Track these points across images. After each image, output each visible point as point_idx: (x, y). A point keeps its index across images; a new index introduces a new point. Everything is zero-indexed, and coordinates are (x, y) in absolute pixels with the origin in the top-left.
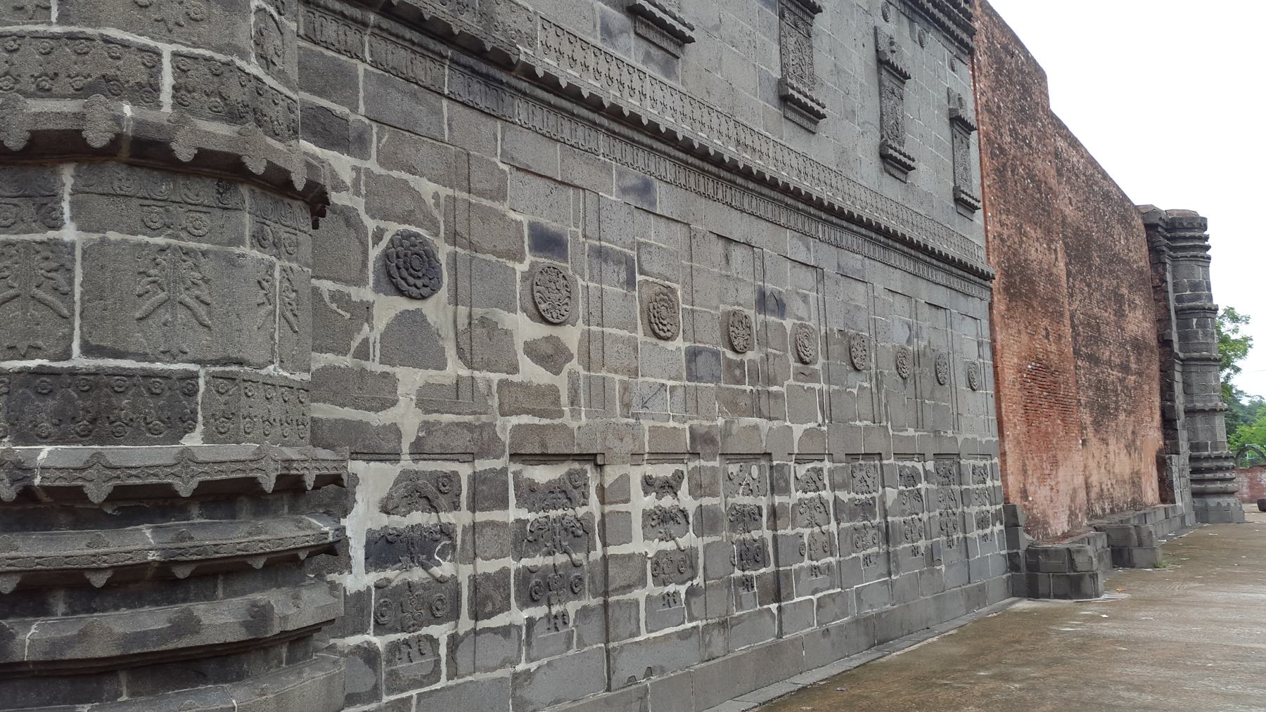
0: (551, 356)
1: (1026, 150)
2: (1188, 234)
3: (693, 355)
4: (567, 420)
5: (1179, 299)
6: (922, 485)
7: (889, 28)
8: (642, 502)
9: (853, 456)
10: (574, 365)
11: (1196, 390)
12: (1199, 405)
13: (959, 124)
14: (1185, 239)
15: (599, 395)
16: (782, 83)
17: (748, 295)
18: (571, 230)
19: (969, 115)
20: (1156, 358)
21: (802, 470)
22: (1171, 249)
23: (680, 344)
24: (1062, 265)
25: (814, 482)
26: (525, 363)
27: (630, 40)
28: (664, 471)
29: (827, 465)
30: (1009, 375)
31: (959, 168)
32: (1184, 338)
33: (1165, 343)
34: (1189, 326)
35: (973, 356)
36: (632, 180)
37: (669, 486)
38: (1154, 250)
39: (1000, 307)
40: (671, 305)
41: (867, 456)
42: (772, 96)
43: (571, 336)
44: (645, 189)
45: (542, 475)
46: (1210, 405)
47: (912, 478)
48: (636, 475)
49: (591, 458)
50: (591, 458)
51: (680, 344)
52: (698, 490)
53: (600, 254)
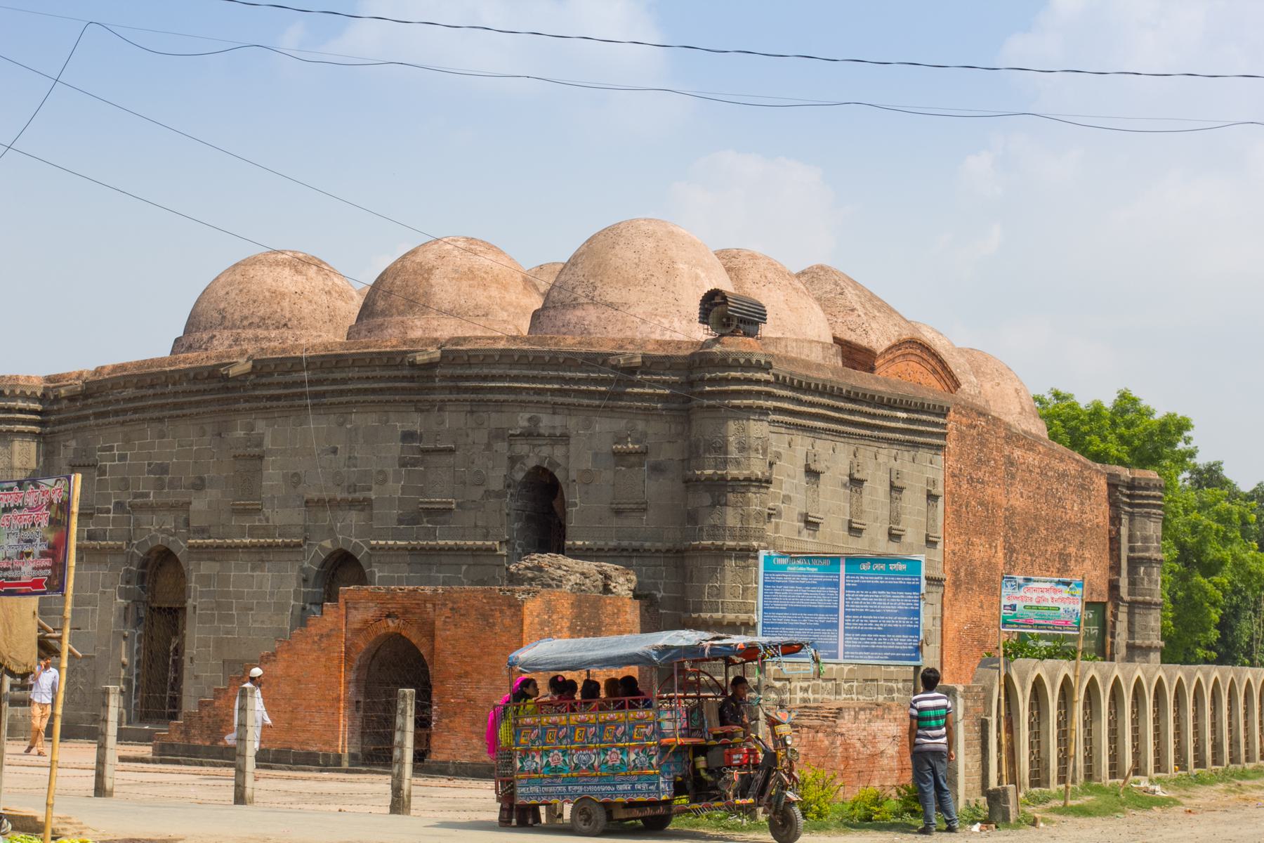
1: (979, 486)
2: (1145, 493)
5: (1132, 549)
6: (895, 695)
7: (896, 465)
8: (800, 695)
9: (866, 680)
11: (1137, 629)
12: (1138, 642)
13: (932, 497)
14: (1142, 497)
19: (939, 490)
21: (846, 686)
22: (1130, 505)
24: (1000, 554)
25: (850, 691)
27: (805, 532)
28: (805, 684)
29: (855, 684)
30: (950, 635)
31: (930, 521)
32: (1132, 583)
34: (1137, 573)
35: (929, 626)
37: (806, 690)
38: (1114, 504)
39: (949, 595)
41: (872, 680)
45: (778, 684)
46: (1147, 642)
47: (890, 691)
48: (799, 684)
49: (788, 680)
50: (788, 680)
52: (814, 692)
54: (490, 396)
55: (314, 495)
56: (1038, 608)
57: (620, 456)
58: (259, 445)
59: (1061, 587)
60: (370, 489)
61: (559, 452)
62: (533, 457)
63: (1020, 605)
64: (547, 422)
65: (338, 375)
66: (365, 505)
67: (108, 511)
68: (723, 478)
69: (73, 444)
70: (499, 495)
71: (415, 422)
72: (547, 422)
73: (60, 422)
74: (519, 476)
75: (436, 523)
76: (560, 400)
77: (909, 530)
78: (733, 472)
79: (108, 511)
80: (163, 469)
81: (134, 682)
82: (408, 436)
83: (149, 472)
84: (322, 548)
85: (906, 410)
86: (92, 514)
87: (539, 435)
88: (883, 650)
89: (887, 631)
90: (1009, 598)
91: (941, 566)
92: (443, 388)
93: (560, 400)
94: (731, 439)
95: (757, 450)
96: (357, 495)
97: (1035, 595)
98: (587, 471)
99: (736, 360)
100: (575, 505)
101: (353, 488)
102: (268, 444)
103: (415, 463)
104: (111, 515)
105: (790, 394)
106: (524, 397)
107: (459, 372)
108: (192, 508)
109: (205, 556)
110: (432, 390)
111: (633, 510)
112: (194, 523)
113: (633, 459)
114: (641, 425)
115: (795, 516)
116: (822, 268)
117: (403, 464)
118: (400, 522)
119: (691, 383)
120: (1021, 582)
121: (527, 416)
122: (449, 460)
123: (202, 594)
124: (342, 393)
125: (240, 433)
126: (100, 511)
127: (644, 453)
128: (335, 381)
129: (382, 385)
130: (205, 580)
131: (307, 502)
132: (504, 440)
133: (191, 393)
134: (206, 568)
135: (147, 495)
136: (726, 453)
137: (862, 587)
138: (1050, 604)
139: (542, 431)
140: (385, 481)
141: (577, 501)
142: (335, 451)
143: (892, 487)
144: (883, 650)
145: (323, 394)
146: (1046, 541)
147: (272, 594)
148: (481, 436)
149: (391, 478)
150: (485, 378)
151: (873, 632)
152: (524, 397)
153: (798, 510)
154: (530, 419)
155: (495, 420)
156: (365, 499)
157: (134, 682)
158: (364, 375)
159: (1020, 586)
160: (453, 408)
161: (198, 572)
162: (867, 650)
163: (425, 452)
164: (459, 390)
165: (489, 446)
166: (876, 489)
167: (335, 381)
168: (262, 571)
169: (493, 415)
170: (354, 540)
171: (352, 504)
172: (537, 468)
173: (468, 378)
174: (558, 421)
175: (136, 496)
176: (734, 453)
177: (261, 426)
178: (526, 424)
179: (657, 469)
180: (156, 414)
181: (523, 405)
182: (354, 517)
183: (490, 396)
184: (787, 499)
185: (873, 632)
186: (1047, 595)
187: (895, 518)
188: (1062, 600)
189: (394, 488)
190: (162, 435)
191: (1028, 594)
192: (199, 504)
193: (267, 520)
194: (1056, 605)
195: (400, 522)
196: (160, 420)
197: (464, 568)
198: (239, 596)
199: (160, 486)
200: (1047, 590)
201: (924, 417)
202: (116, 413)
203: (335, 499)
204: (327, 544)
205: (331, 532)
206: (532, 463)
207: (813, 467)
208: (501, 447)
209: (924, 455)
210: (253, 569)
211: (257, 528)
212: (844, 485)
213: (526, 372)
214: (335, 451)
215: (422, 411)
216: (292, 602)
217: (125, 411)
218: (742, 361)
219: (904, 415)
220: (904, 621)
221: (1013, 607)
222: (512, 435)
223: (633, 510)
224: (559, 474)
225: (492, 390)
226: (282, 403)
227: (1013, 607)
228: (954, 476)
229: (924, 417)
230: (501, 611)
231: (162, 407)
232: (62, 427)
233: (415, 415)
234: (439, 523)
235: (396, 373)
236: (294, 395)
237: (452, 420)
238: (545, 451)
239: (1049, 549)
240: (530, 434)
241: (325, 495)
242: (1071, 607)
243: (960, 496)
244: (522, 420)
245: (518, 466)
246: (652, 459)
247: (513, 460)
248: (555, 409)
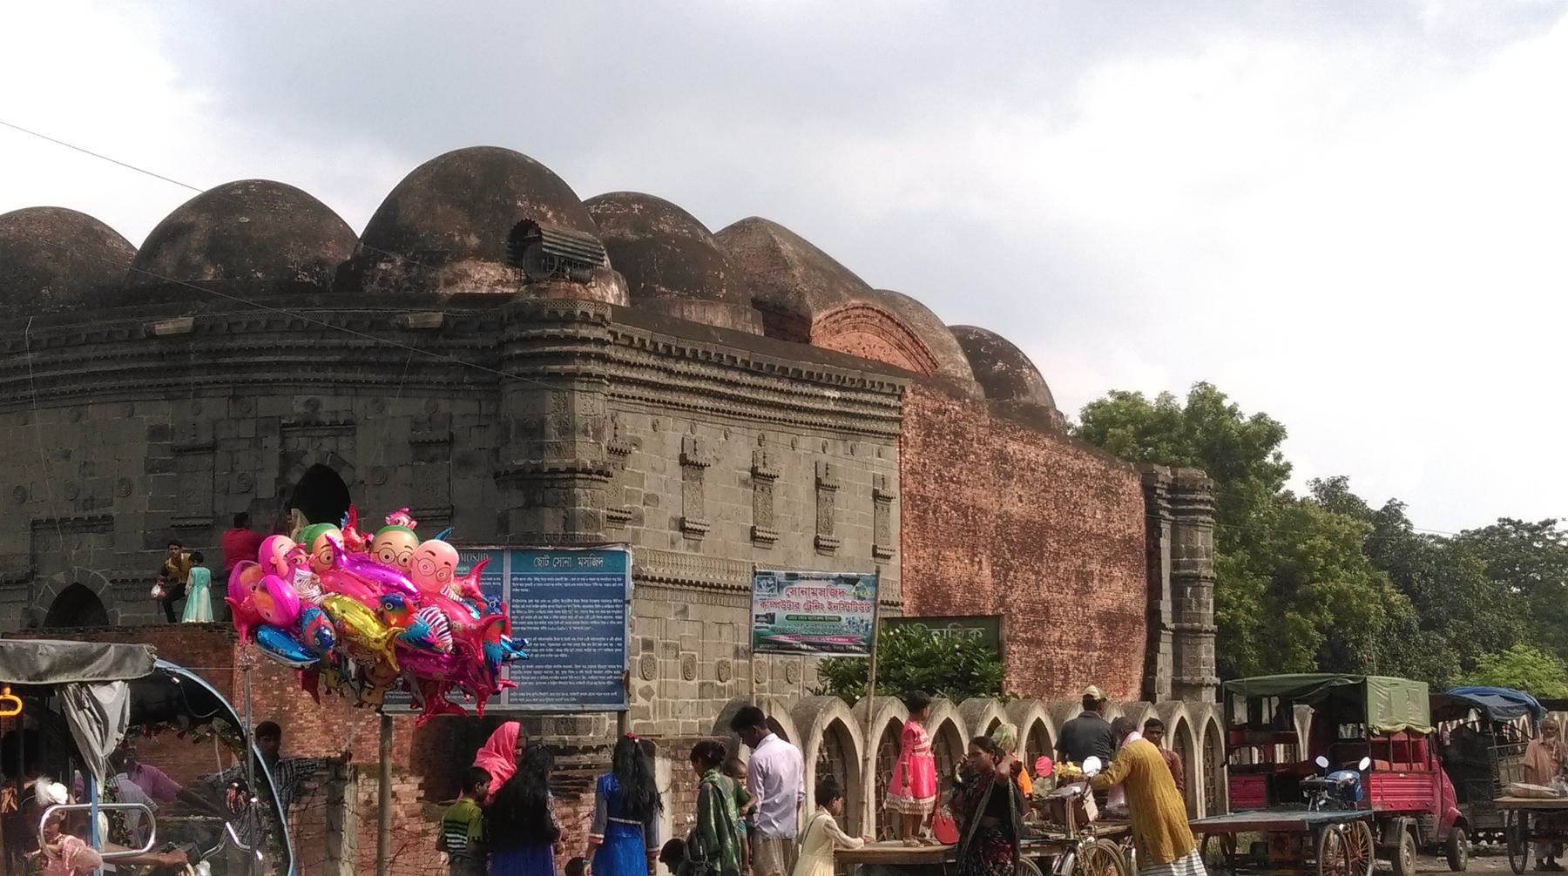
0: (647, 694)
1: (953, 486)
2: (1190, 496)
3: (702, 686)
4: (652, 721)
7: (824, 458)
10: (655, 697)
11: (1184, 663)
12: (1186, 679)
15: (663, 709)
16: (753, 529)
17: (730, 650)
18: (656, 638)
20: (1144, 628)
23: (696, 681)
24: (987, 572)
26: (639, 698)
31: (880, 529)
32: (1178, 607)
33: (1153, 613)
36: (679, 608)
40: (693, 665)
42: (748, 537)
43: (654, 684)
44: (685, 611)
51: (696, 681)
53: (666, 645)
54: (256, 376)
55: (44, 515)
56: (807, 619)
57: (418, 446)
59: (841, 587)
60: (111, 504)
61: (344, 444)
63: (781, 615)
64: (329, 406)
65: (69, 355)
66: (104, 524)
68: (538, 470)
71: (164, 413)
72: (329, 406)
74: (295, 478)
76: (341, 376)
77: (847, 541)
78: (551, 461)
82: (157, 433)
84: (52, 583)
85: (838, 388)
87: (319, 424)
88: (569, 689)
89: (574, 658)
90: (763, 605)
91: (897, 587)
92: (200, 367)
93: (341, 376)
94: (549, 418)
95: (586, 432)
96: (94, 513)
97: (802, 600)
98: (375, 469)
99: (555, 312)
101: (91, 502)
105: (651, 361)
106: (300, 374)
107: (218, 345)
110: (186, 369)
113: (434, 450)
114: (444, 406)
115: (665, 521)
116: (755, 220)
117: (151, 468)
118: (148, 545)
119: (501, 345)
120: (783, 580)
121: (305, 398)
122: (209, 460)
124: (75, 378)
127: (451, 441)
128: (66, 363)
129: (125, 366)
131: (34, 523)
136: (543, 434)
137: (539, 593)
138: (828, 614)
140: (128, 493)
142: (67, 456)
143: (818, 484)
144: (569, 689)
145: (53, 381)
146: (1058, 556)
148: (247, 429)
150: (251, 351)
151: (553, 661)
152: (300, 374)
153: (670, 514)
155: (266, 406)
158: (101, 353)
159: (780, 586)
162: (544, 689)
163: (180, 451)
164: (219, 368)
166: (794, 487)
167: (66, 363)
169: (262, 401)
171: (90, 524)
172: (317, 467)
173: (230, 352)
174: (342, 403)
176: (552, 435)
178: (302, 410)
179: (465, 463)
183: (256, 376)
184: (651, 499)
185: (553, 661)
186: (822, 600)
187: (825, 524)
188: (845, 606)
191: (793, 599)
194: (836, 614)
195: (148, 545)
200: (822, 591)
201: (867, 397)
203: (68, 519)
204: (60, 578)
206: (310, 460)
207: (690, 458)
209: (867, 446)
212: (744, 483)
213: (300, 342)
214: (67, 456)
218: (562, 313)
219: (837, 394)
220: (600, 643)
221: (770, 618)
222: (285, 426)
224: (345, 477)
225: (259, 366)
227: (770, 618)
228: (913, 472)
229: (867, 397)
230: (206, 656)
235: (142, 350)
236: (15, 385)
237: (214, 407)
238: (328, 445)
239: (1062, 565)
240: (309, 424)
241: (56, 516)
242: (857, 616)
243: (924, 499)
244: (297, 405)
247: (287, 460)
248: (337, 388)
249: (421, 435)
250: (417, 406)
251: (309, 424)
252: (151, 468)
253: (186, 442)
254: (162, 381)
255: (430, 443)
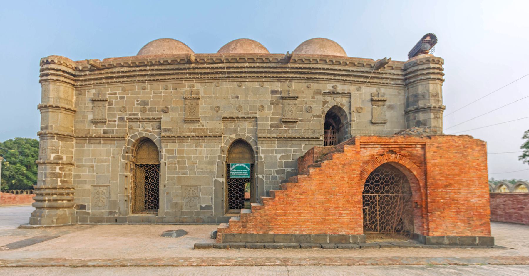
55: (228, 116)
58: (198, 94)
60: (256, 113)
62: (332, 102)
64: (340, 88)
67: (115, 121)
69: (94, 91)
70: (319, 116)
71: (278, 86)
72: (340, 88)
73: (86, 80)
74: (326, 110)
75: (289, 127)
79: (115, 121)
80: (145, 103)
81: (130, 197)
82: (274, 92)
83: (137, 104)
84: (230, 138)
86: (105, 122)
87: (337, 93)
100: (354, 121)
102: (202, 94)
103: (278, 103)
104: (117, 123)
108: (162, 120)
109: (170, 141)
111: (381, 123)
112: (163, 127)
114: (383, 90)
117: (272, 103)
118: (271, 127)
123: (169, 158)
125: (187, 89)
126: (109, 121)
130: (168, 151)
132: (320, 94)
133: (161, 70)
134: (170, 146)
135: (137, 114)
139: (338, 91)
141: (355, 119)
147: (207, 157)
149: (266, 108)
154: (333, 87)
156: (253, 118)
157: (130, 197)
160: (296, 81)
161: (165, 148)
163: (282, 98)
165: (313, 97)
168: (201, 147)
169: (316, 84)
170: (247, 135)
175: (130, 115)
177: (198, 86)
178: (331, 89)
179: (391, 107)
180: (141, 79)
181: (329, 80)
182: (247, 125)
189: (268, 113)
190: (144, 89)
192: (165, 118)
193: (203, 126)
195: (271, 127)
196: (143, 81)
197: (303, 146)
198: (189, 158)
199: (144, 111)
202: (118, 77)
204: (234, 136)
205: (235, 131)
208: (320, 97)
210: (196, 146)
211: (198, 129)
214: (237, 97)
215: (281, 82)
216: (218, 160)
217: (123, 77)
222: (324, 93)
223: (381, 123)
226: (209, 76)
231: (145, 75)
232: (87, 83)
233: (277, 83)
234: (291, 128)
240: (333, 93)
244: (329, 87)
245: (326, 105)
246: (387, 103)
249: (375, 98)
250: (374, 90)
251: (333, 93)
252: (272, 103)
253: (286, 95)
254: (279, 75)
255: (381, 100)
